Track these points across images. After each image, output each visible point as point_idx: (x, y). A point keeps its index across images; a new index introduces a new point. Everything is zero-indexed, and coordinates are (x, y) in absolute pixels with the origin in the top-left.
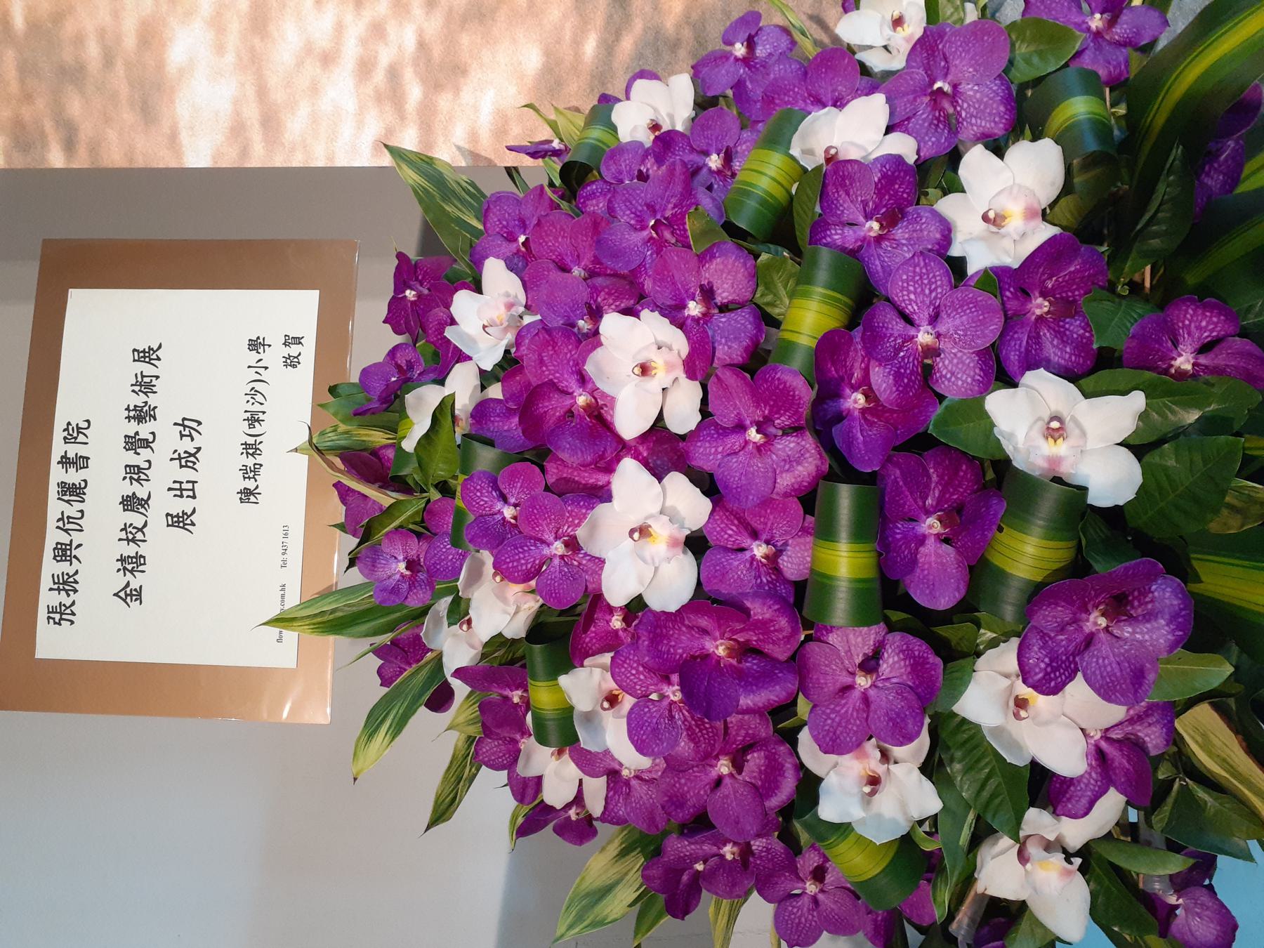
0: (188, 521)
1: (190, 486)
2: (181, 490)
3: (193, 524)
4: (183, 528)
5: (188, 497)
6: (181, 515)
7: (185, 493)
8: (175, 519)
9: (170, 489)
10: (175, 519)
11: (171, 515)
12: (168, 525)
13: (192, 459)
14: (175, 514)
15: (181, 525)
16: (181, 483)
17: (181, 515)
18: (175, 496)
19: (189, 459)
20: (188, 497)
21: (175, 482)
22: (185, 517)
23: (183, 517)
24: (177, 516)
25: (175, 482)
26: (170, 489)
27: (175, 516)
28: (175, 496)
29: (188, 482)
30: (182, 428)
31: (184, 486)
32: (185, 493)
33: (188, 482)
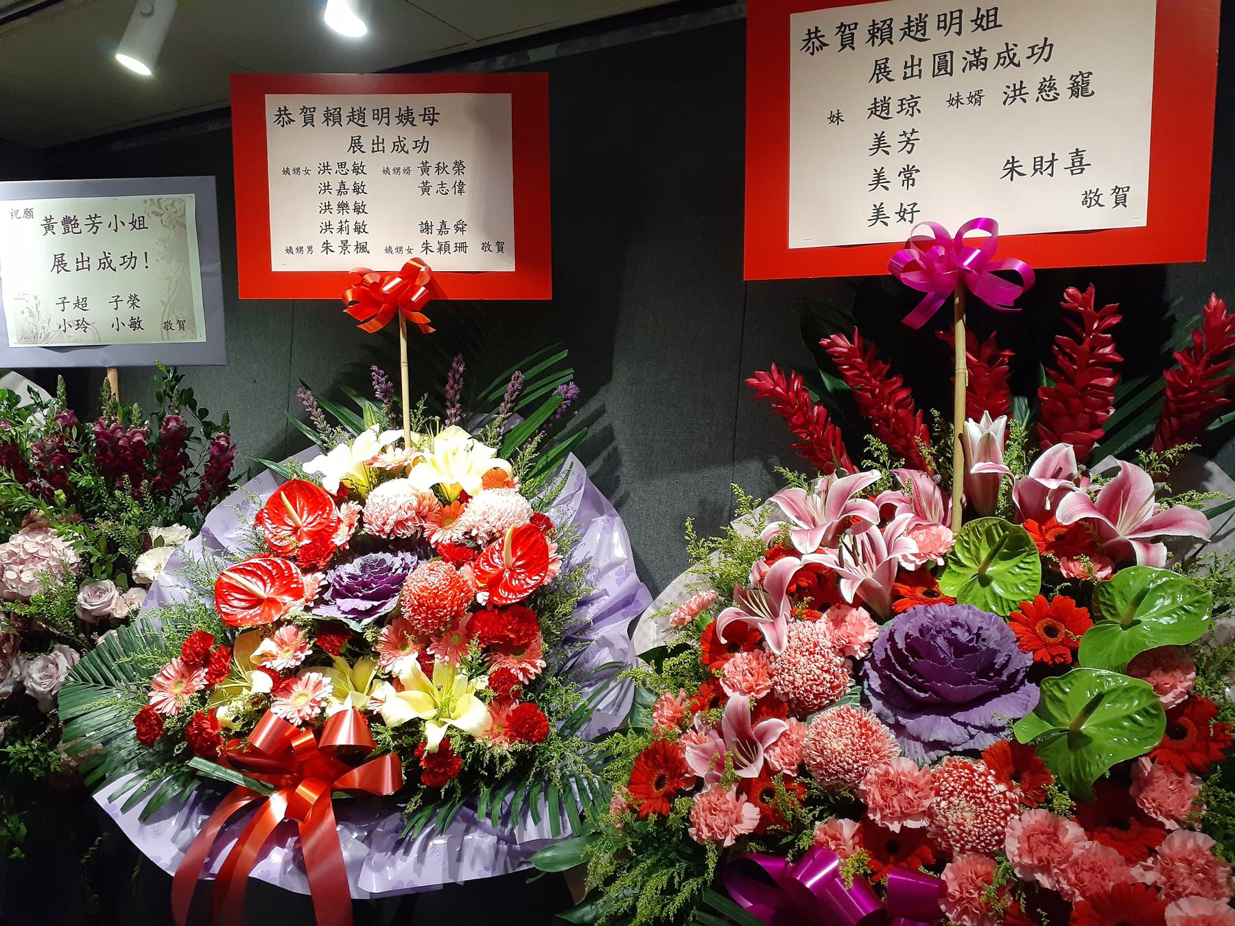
0: (880, 77)
1: (916, 72)
2: (912, 66)
3: (878, 81)
4: (874, 73)
5: (905, 73)
6: (887, 70)
7: (909, 71)
8: (883, 66)
9: (912, 57)
10: (883, 66)
11: (887, 62)
12: (876, 61)
13: (1008, 61)
14: (888, 65)
15: (878, 72)
16: (919, 65)
17: (887, 70)
18: (906, 62)
19: (1007, 59)
20: (905, 73)
21: (920, 60)
22: (885, 74)
23: (885, 72)
24: (886, 67)
25: (920, 60)
26: (912, 57)
27: (885, 66)
28: (906, 62)
29: (920, 70)
30: (1041, 45)
31: (916, 69)
32: (909, 71)
33: (920, 70)
